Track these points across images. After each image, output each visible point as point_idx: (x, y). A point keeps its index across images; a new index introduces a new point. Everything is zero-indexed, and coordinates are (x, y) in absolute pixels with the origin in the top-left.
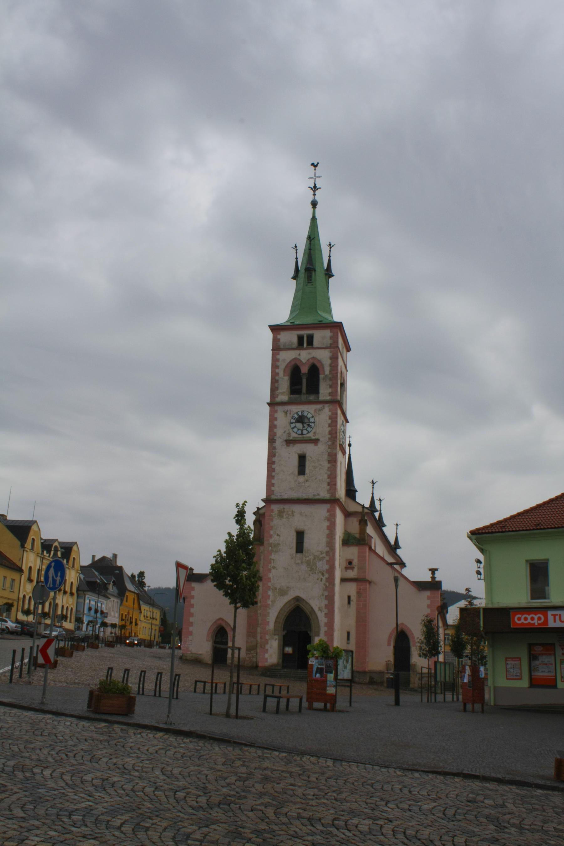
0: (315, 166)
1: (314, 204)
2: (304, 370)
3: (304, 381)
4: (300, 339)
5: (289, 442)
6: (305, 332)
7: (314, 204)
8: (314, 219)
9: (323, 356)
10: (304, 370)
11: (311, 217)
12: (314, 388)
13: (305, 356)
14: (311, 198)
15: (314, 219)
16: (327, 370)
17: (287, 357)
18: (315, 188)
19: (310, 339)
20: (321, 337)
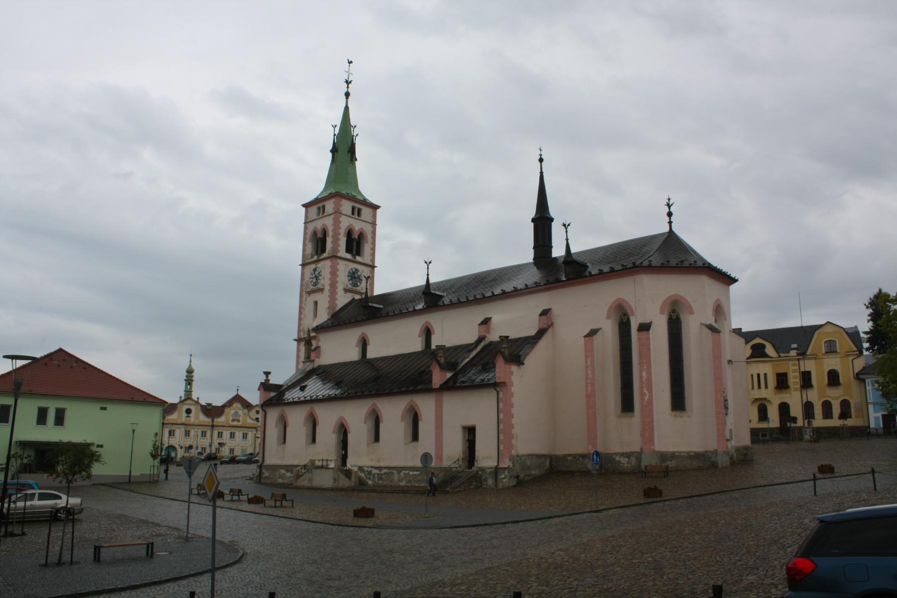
0: (350, 62)
1: (347, 95)
2: (356, 236)
3: (355, 243)
4: (353, 208)
5: (346, 290)
6: (358, 206)
7: (347, 95)
8: (347, 108)
9: (368, 229)
10: (355, 236)
11: (344, 105)
12: (358, 253)
13: (357, 226)
14: (346, 90)
15: (347, 108)
16: (370, 240)
17: (346, 222)
18: (348, 82)
19: (359, 211)
20: (366, 212)
